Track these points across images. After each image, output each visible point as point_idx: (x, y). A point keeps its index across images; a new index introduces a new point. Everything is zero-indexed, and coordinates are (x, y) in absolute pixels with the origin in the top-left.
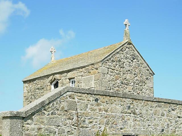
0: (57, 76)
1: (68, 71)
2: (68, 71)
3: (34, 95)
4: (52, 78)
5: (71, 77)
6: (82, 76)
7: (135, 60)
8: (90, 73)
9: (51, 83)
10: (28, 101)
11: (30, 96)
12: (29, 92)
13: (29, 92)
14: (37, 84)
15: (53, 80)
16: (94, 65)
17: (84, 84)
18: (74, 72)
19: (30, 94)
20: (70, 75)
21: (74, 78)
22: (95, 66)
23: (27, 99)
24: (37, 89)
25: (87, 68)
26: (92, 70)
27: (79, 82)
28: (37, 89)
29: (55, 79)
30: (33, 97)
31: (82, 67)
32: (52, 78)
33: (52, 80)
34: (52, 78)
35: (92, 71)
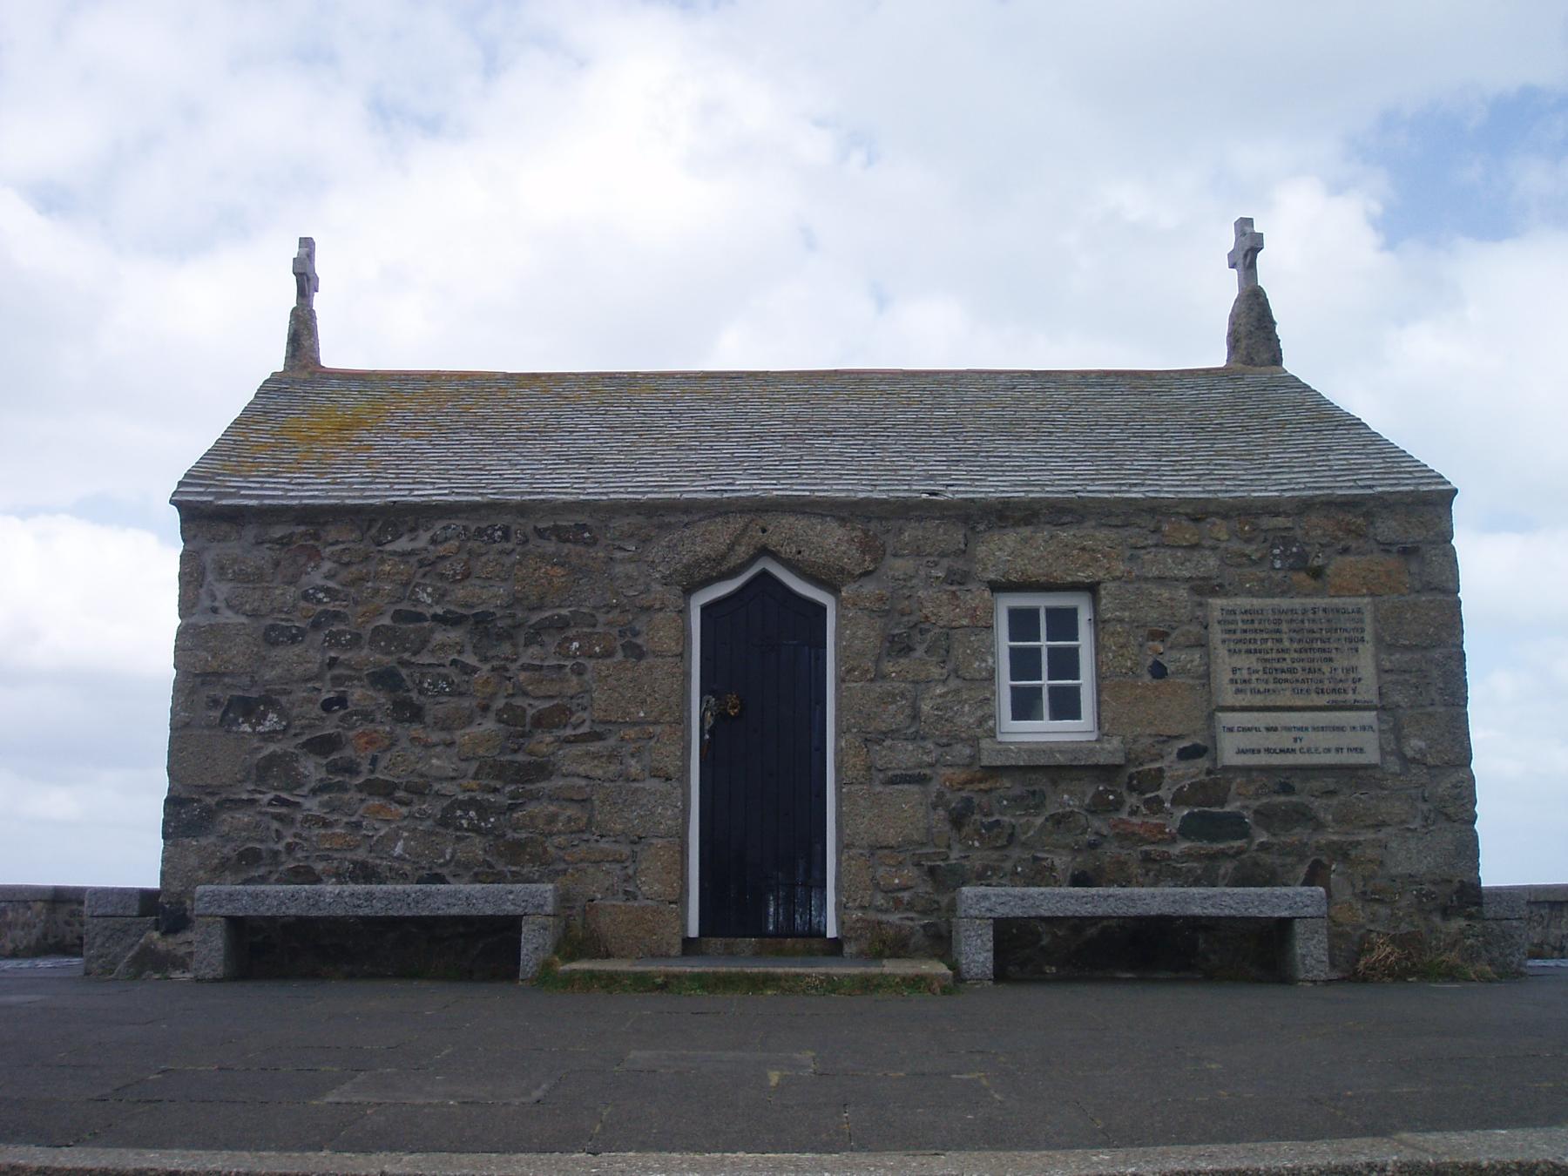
2: (1004, 514)
3: (385, 679)
4: (731, 547)
6: (1204, 588)
8: (1317, 573)
9: (689, 591)
11: (318, 677)
16: (1368, 515)
17: (1243, 661)
20: (1001, 551)
22: (1387, 528)
23: (247, 708)
25: (1267, 522)
27: (1162, 636)
31: (1199, 512)
35: (1339, 566)
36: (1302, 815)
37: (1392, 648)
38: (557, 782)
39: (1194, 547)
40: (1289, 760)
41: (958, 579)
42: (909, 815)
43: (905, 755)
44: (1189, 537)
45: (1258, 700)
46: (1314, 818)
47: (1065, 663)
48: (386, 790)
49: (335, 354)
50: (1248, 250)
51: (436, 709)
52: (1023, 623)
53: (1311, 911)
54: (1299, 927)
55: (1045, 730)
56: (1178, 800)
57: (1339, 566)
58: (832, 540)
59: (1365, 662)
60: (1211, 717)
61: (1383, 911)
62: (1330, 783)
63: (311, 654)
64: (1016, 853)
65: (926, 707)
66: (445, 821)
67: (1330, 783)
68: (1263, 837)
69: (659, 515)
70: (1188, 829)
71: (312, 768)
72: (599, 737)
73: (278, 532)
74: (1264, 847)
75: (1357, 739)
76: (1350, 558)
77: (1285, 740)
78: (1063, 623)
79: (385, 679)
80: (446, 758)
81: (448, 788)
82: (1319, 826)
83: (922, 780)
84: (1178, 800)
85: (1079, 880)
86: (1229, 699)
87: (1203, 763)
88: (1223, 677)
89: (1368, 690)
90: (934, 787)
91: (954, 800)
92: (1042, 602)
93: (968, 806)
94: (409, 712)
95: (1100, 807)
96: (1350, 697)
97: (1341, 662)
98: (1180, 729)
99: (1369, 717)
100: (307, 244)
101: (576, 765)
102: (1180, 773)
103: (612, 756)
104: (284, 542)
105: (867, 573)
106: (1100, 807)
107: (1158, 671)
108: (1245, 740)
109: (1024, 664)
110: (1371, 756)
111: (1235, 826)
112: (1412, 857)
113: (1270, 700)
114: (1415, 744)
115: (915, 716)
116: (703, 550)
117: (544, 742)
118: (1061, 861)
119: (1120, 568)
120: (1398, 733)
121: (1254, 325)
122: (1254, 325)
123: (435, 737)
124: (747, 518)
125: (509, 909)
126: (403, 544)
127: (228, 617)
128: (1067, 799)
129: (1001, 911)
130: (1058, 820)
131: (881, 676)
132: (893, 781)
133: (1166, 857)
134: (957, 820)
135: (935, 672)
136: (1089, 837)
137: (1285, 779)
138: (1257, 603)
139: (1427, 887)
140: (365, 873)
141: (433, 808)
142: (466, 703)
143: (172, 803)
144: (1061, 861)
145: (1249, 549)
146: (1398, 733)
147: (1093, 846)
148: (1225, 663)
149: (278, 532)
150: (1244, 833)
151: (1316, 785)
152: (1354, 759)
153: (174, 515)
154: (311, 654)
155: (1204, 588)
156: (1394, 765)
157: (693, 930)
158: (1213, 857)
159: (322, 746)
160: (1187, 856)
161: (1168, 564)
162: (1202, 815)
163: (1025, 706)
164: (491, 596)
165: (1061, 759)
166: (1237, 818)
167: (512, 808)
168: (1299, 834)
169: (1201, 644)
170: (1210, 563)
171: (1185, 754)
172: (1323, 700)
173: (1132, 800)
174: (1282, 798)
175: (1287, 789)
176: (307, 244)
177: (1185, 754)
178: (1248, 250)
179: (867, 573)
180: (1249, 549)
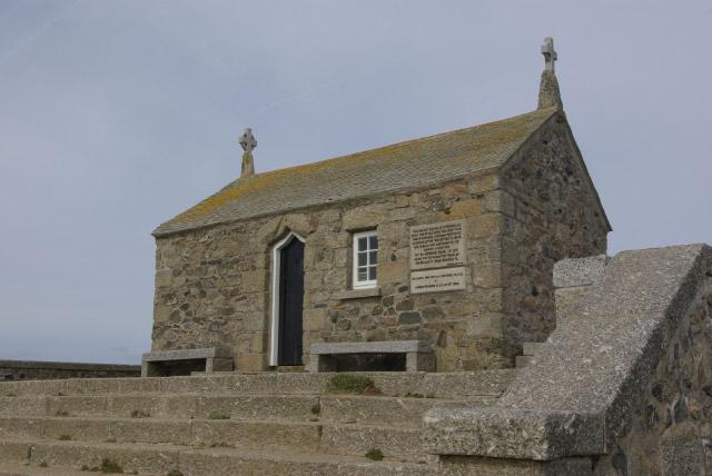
0: (299, 222)
1: (350, 203)
2: (350, 203)
3: (198, 284)
4: (278, 228)
5: (356, 224)
6: (411, 222)
7: (571, 179)
8: (447, 212)
9: (272, 244)
10: (174, 302)
12: (177, 273)
13: (177, 273)
14: (213, 246)
15: (279, 233)
16: (467, 183)
17: (421, 251)
18: (377, 207)
19: (184, 279)
20: (352, 218)
21: (374, 228)
22: (473, 188)
23: (169, 297)
24: (212, 263)
25: (432, 192)
26: (458, 200)
27: (395, 244)
28: (212, 263)
29: (287, 230)
30: (194, 291)
32: (278, 228)
33: (276, 232)
34: (275, 226)
35: (456, 207)
36: (438, 312)
37: (472, 239)
38: (236, 314)
39: (408, 206)
40: (433, 289)
41: (338, 230)
44: (406, 204)
45: (423, 266)
46: (442, 313)
48: (197, 320)
51: (209, 292)
52: (362, 243)
53: (411, 350)
54: (408, 356)
56: (399, 308)
57: (456, 207)
59: (461, 247)
60: (409, 275)
61: (464, 350)
62: (448, 298)
63: (181, 280)
64: (352, 331)
65: (325, 279)
67: (448, 298)
68: (425, 321)
70: (406, 318)
71: (183, 314)
72: (245, 298)
73: (177, 239)
74: (426, 326)
76: (460, 202)
77: (431, 282)
79: (198, 284)
80: (209, 308)
81: (211, 318)
82: (444, 316)
83: (324, 306)
84: (399, 308)
85: (369, 340)
86: (414, 267)
87: (406, 293)
88: (413, 257)
89: (461, 258)
90: (327, 309)
91: (333, 312)
92: (367, 235)
93: (337, 315)
94: (203, 294)
95: (376, 312)
96: (455, 261)
97: (452, 247)
98: (398, 280)
99: (461, 270)
101: (239, 307)
102: (399, 297)
103: (247, 305)
104: (178, 243)
105: (312, 232)
106: (376, 312)
107: (394, 258)
108: (419, 283)
109: (362, 260)
110: (462, 286)
111: (416, 317)
113: (431, 265)
114: (478, 279)
115: (323, 282)
116: (270, 230)
117: (232, 301)
118: (364, 334)
119: (383, 218)
120: (472, 275)
123: (209, 302)
124: (280, 217)
125: (200, 356)
126: (203, 240)
127: (167, 269)
129: (321, 352)
130: (363, 318)
131: (314, 269)
132: (317, 307)
133: (395, 331)
134: (334, 321)
135: (330, 266)
136: (373, 324)
137: (433, 297)
138: (425, 226)
139: (480, 340)
140: (193, 347)
141: (208, 326)
142: (216, 290)
143: (155, 328)
144: (364, 334)
145: (424, 204)
146: (472, 275)
147: (374, 328)
148: (414, 251)
149: (177, 239)
150: (418, 321)
151: (443, 300)
152: (455, 287)
153: (154, 239)
155: (411, 222)
156: (470, 289)
157: (273, 361)
158: (410, 330)
159: (185, 307)
160: (401, 331)
161: (398, 215)
162: (407, 314)
163: (362, 278)
164: (220, 254)
165: (360, 295)
166: (417, 314)
167: (226, 323)
168: (438, 320)
169: (408, 246)
170: (412, 213)
171: (402, 290)
172: (445, 264)
173: (385, 309)
174: (432, 305)
175: (434, 302)
177: (402, 290)
179: (312, 232)
180: (424, 204)
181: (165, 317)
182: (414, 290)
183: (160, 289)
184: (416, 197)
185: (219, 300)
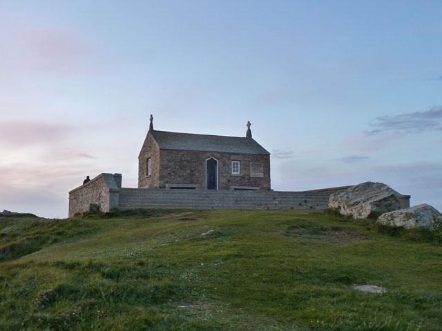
2: (234, 154)
6: (249, 161)
13: (169, 161)
20: (233, 157)
23: (167, 168)
41: (229, 159)
42: (225, 180)
43: (224, 175)
47: (237, 167)
49: (155, 129)
50: (249, 125)
52: (234, 163)
55: (235, 173)
58: (219, 155)
59: (262, 168)
66: (185, 180)
69: (204, 152)
75: (262, 176)
78: (237, 164)
94: (181, 169)
100: (151, 115)
101: (197, 174)
102: (247, 177)
106: (241, 180)
112: (265, 186)
121: (249, 133)
122: (249, 133)
128: (238, 179)
140: (178, 184)
148: (251, 168)
154: (173, 164)
155: (249, 161)
159: (174, 172)
163: (234, 171)
164: (189, 159)
176: (151, 115)
178: (249, 125)
181: (165, 173)
182: (251, 176)
183: (162, 166)
184: (251, 156)
185: (188, 171)
